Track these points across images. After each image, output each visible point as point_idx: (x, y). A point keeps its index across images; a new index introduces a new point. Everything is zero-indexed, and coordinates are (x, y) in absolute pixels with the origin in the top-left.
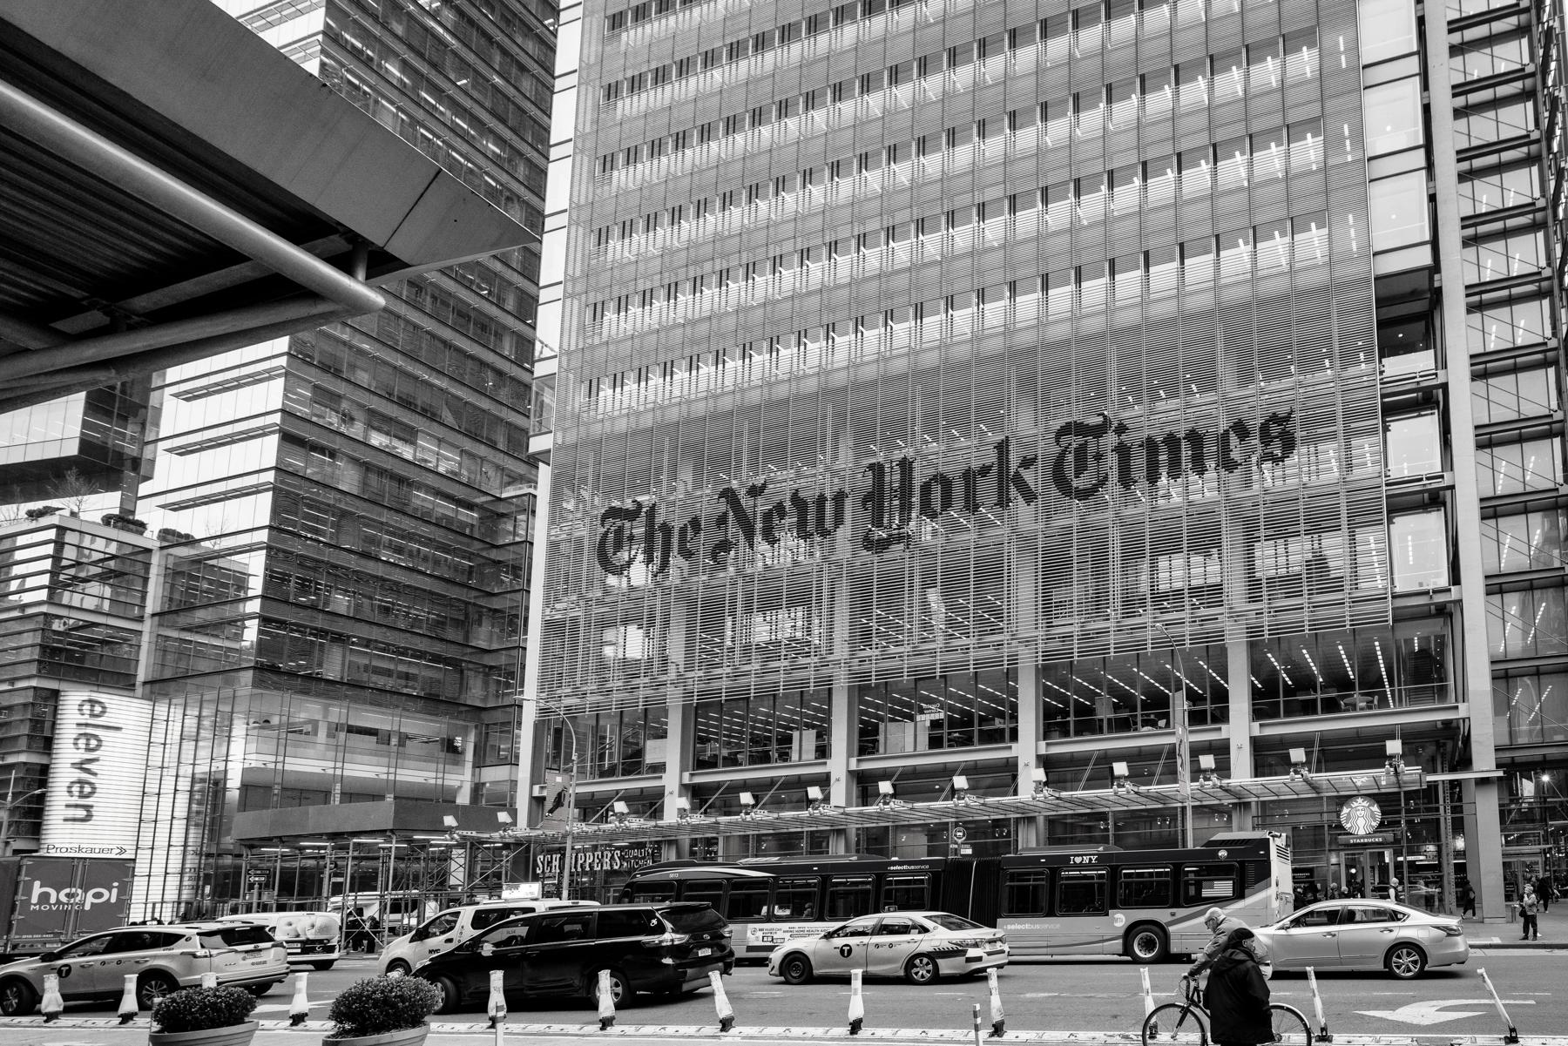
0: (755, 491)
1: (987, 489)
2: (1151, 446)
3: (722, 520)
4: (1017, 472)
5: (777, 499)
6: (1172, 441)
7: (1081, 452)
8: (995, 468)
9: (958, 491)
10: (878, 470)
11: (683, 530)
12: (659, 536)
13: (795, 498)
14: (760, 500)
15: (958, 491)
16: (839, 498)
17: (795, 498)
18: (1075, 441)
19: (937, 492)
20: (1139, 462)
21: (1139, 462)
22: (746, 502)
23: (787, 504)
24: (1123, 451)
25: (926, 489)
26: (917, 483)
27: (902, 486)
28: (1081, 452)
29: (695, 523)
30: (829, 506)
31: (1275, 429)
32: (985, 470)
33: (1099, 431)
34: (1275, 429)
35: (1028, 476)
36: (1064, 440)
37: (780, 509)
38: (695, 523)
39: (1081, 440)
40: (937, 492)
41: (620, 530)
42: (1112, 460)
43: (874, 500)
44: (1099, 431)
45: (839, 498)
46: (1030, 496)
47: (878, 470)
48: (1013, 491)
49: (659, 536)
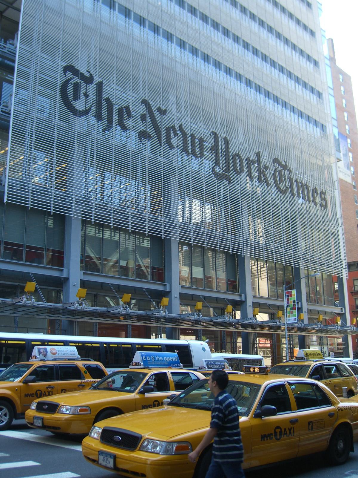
3: (143, 118)
4: (263, 170)
22: (157, 114)
25: (234, 156)
32: (254, 162)
42: (287, 181)
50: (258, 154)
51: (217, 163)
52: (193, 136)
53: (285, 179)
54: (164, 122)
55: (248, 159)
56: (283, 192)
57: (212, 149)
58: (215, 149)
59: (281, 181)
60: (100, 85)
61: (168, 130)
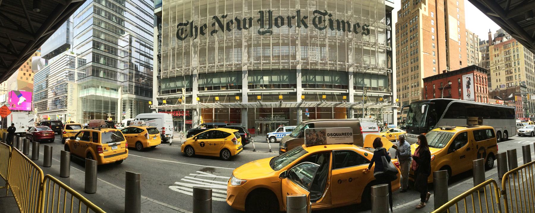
1: (295, 22)
5: (230, 19)
7: (320, 18)
9: (286, 21)
10: (262, 13)
11: (201, 28)
12: (194, 29)
13: (236, 19)
14: (225, 19)
15: (286, 21)
16: (250, 19)
17: (236, 19)
18: (318, 15)
19: (279, 21)
20: (335, 25)
21: (335, 25)
22: (221, 20)
23: (234, 21)
24: (331, 21)
25: (276, 20)
26: (273, 18)
27: (269, 18)
28: (320, 18)
29: (205, 26)
30: (247, 21)
32: (294, 17)
33: (325, 14)
36: (316, 14)
37: (232, 21)
38: (205, 26)
40: (279, 21)
41: (182, 29)
42: (327, 23)
43: (261, 21)
44: (325, 14)
45: (250, 19)
46: (306, 26)
47: (262, 13)
49: (194, 29)
50: (298, 12)
55: (288, 17)
57: (258, 21)
58: (261, 21)
59: (320, 22)
61: (228, 24)
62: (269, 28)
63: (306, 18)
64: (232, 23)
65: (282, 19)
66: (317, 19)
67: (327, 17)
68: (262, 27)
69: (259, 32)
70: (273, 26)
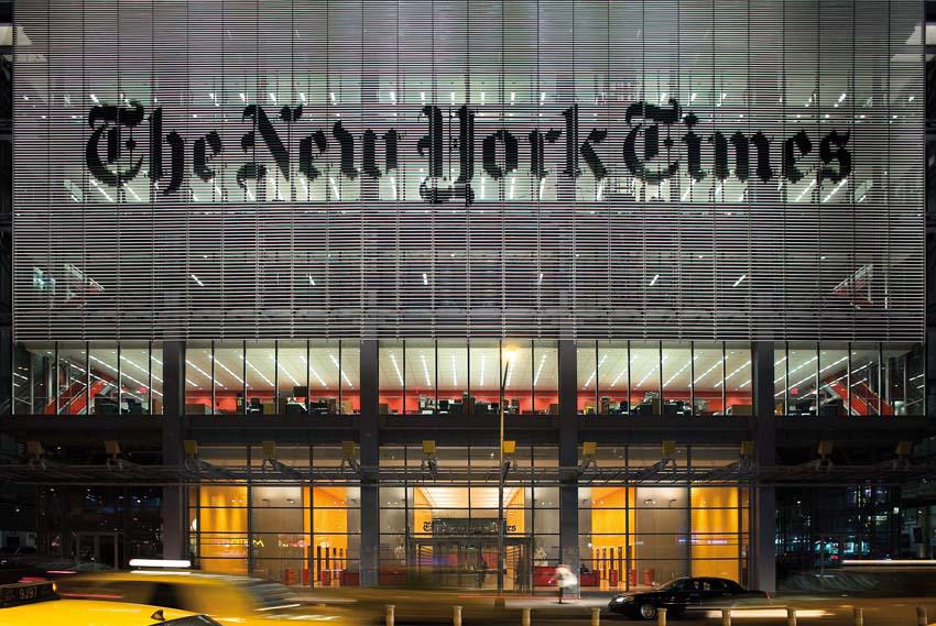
0: (291, 114)
1: (554, 153)
2: (719, 141)
3: (248, 141)
4: (586, 143)
6: (739, 140)
8: (564, 134)
9: (524, 150)
12: (167, 149)
13: (340, 131)
15: (524, 150)
19: (500, 149)
20: (707, 152)
21: (707, 152)
22: (280, 127)
24: (693, 142)
25: (489, 145)
26: (479, 137)
31: (833, 147)
32: (553, 136)
34: (833, 147)
35: (599, 150)
36: (636, 120)
37: (320, 138)
38: (214, 140)
39: (650, 122)
40: (500, 149)
42: (682, 150)
45: (392, 138)
46: (600, 172)
48: (583, 166)
49: (167, 149)
50: (571, 115)
51: (436, 171)
52: (369, 137)
53: (669, 143)
54: (290, 135)
55: (534, 138)
56: (655, 179)
57: (422, 144)
60: (157, 116)
61: (305, 146)
62: (462, 179)
63: (598, 136)
64: (323, 145)
65: (512, 145)
66: (640, 141)
67: (678, 130)
68: (436, 171)
69: (423, 191)
70: (478, 167)
